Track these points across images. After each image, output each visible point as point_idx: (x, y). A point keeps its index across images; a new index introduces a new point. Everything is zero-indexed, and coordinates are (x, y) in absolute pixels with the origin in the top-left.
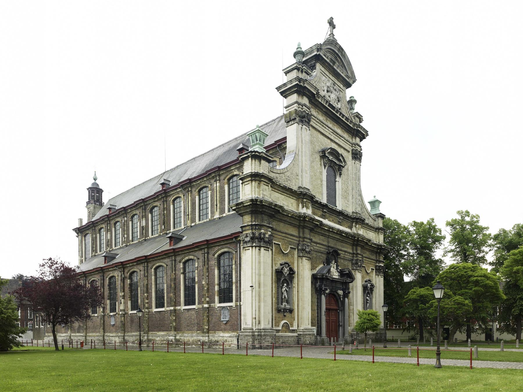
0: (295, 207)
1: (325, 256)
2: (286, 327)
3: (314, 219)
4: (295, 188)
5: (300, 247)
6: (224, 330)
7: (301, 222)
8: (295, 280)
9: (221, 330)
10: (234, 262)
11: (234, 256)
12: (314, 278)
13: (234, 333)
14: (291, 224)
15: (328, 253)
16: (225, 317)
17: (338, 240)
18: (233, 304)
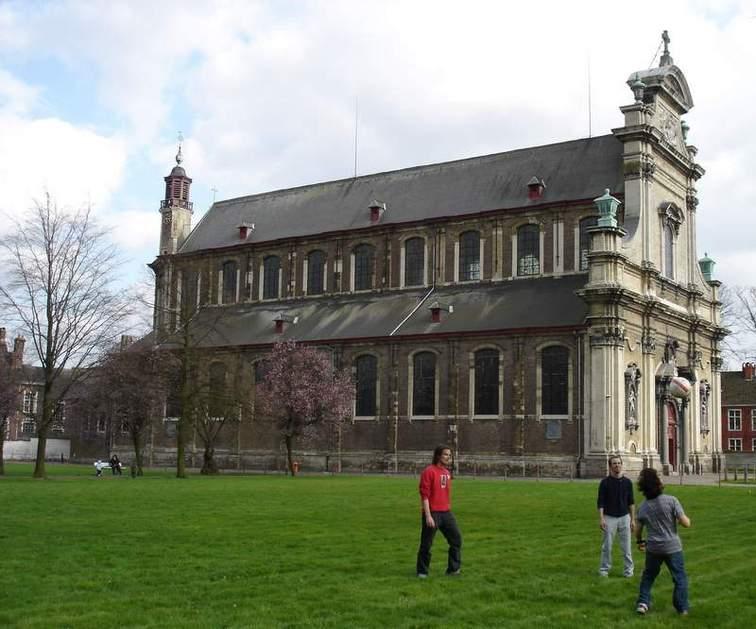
0: (640, 286)
1: (663, 349)
2: (634, 447)
3: (661, 305)
4: (639, 263)
5: (645, 342)
6: (552, 452)
7: (649, 309)
8: (640, 386)
9: (548, 452)
10: (570, 361)
11: (571, 353)
12: (658, 379)
13: (568, 458)
14: (637, 312)
15: (667, 345)
16: (555, 434)
17: (677, 326)
18: (568, 417)
